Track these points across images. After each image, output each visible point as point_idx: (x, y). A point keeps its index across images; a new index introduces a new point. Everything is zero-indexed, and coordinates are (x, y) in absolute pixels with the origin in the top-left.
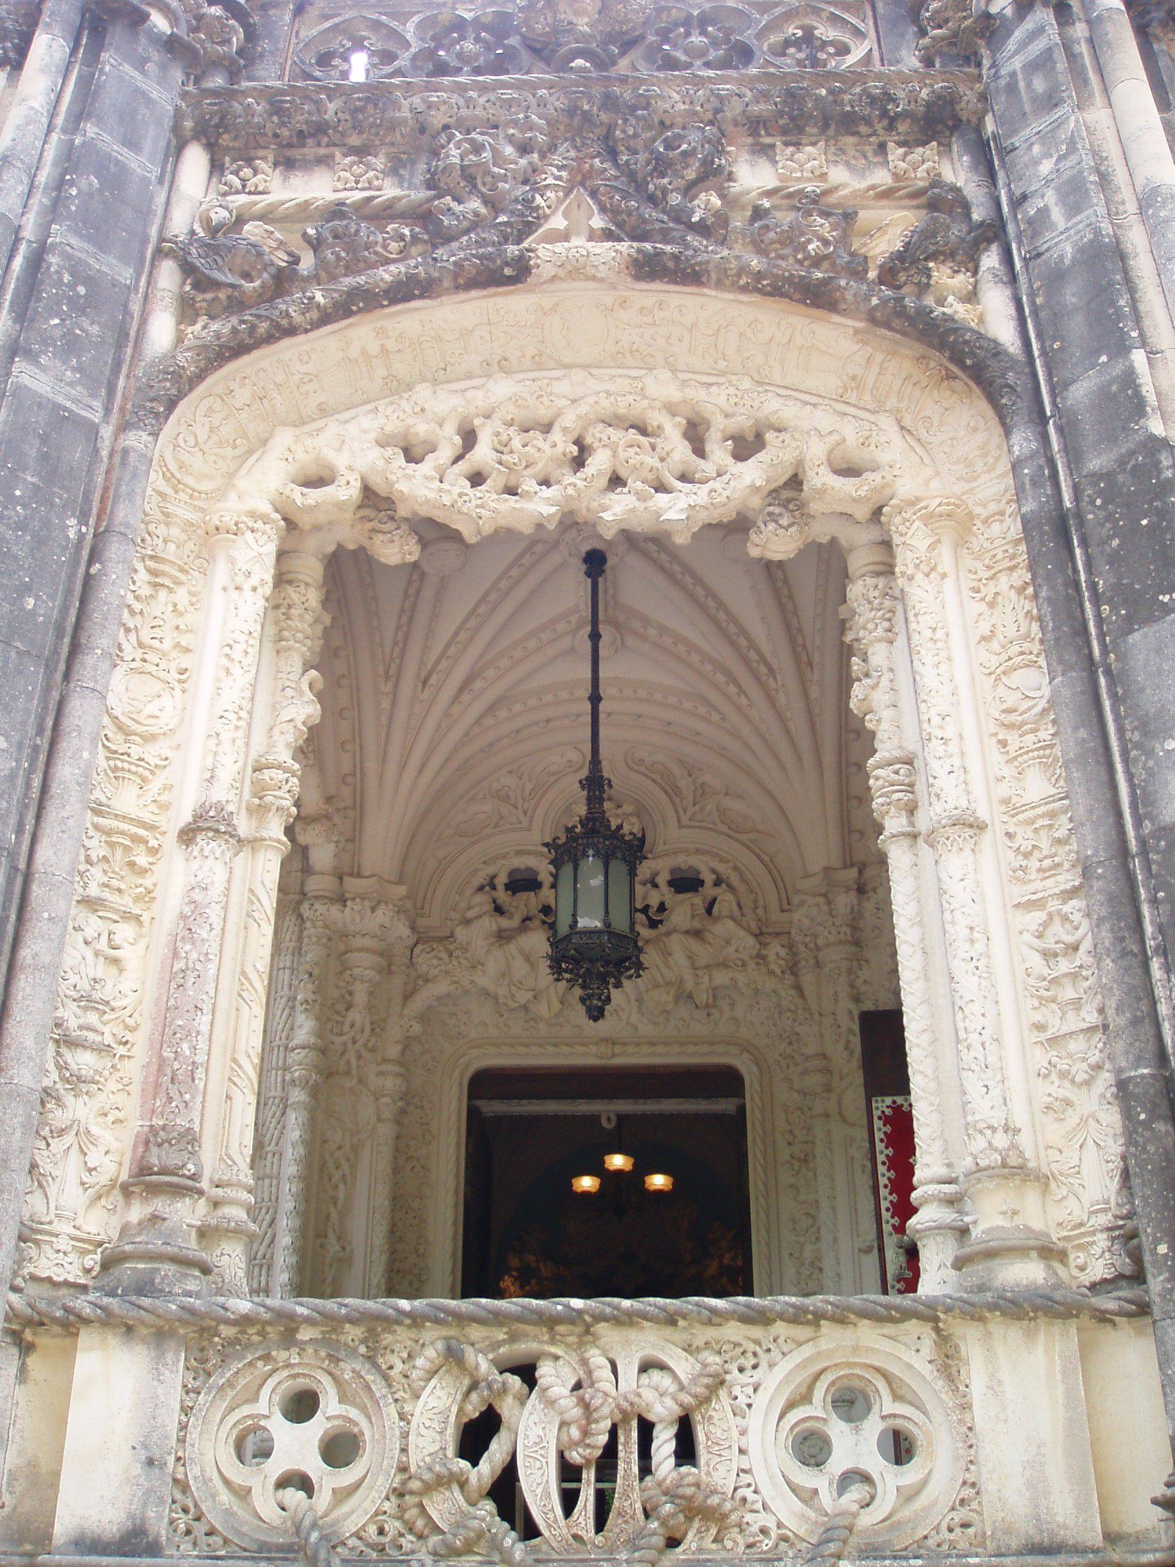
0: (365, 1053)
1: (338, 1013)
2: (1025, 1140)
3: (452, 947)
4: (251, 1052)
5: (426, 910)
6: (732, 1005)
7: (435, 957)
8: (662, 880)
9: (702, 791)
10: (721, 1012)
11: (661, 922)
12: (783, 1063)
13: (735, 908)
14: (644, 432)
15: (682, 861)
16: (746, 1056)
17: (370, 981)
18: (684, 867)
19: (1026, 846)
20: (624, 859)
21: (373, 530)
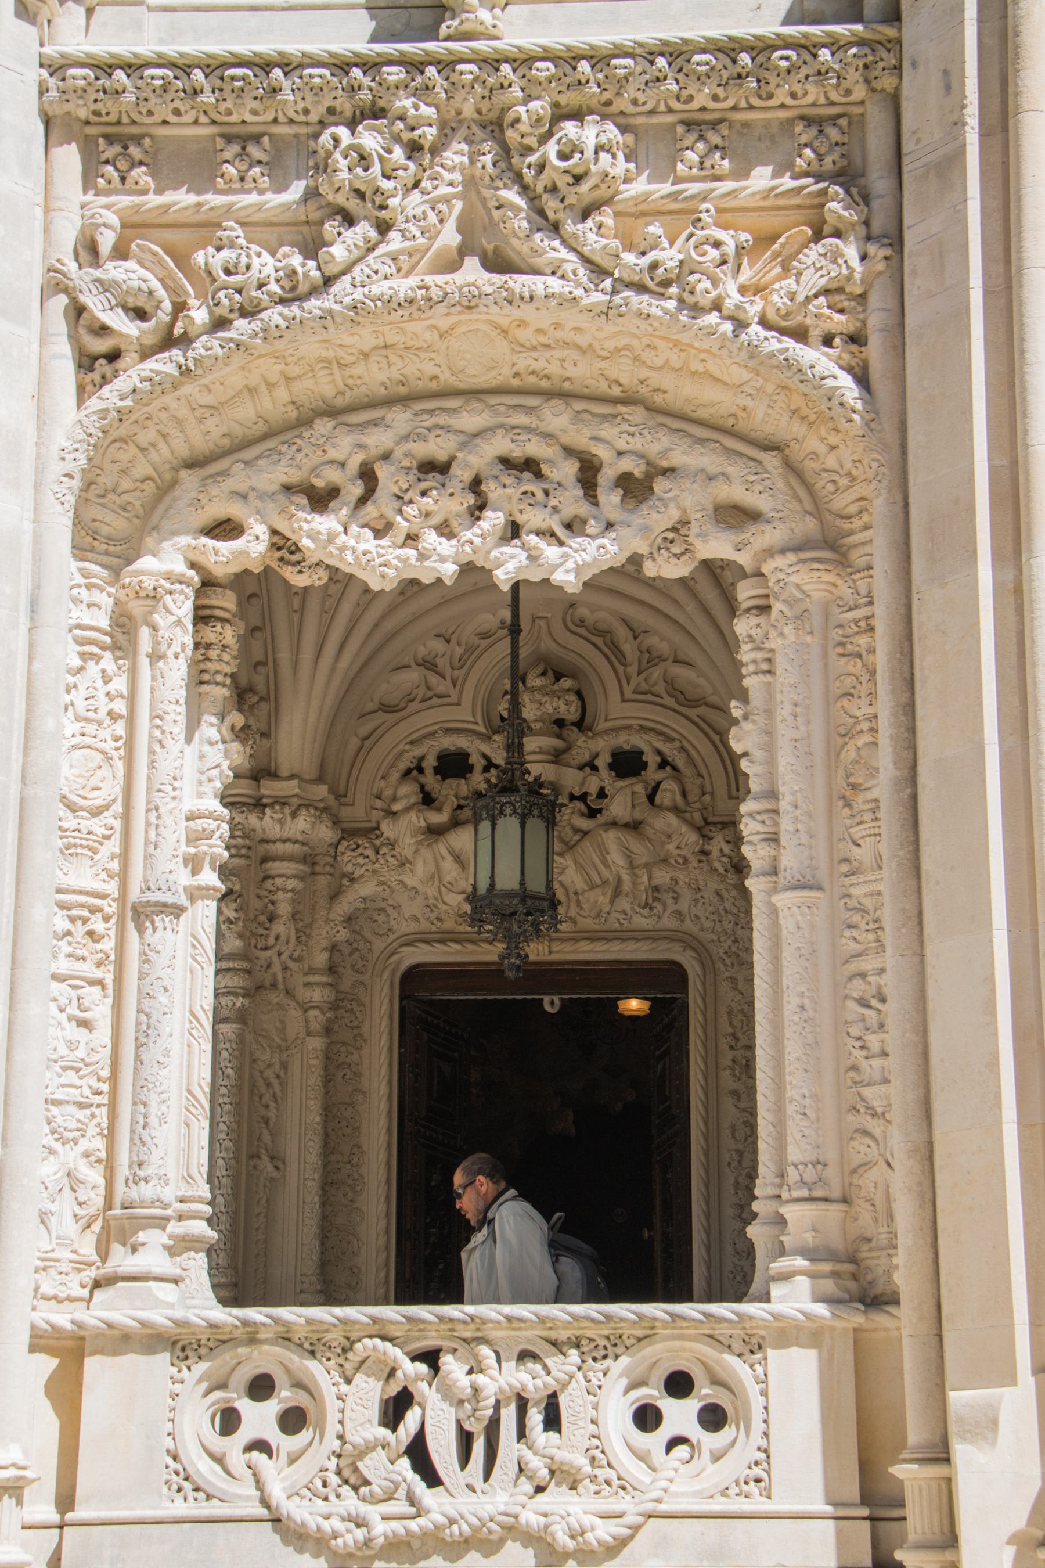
0: (291, 964)
1: (260, 924)
4: (203, 1083)
6: (676, 899)
8: (602, 762)
9: (651, 659)
10: (665, 905)
11: (600, 811)
13: (678, 798)
15: (625, 741)
16: (690, 953)
17: (292, 890)
20: (541, 816)
21: (281, 559)
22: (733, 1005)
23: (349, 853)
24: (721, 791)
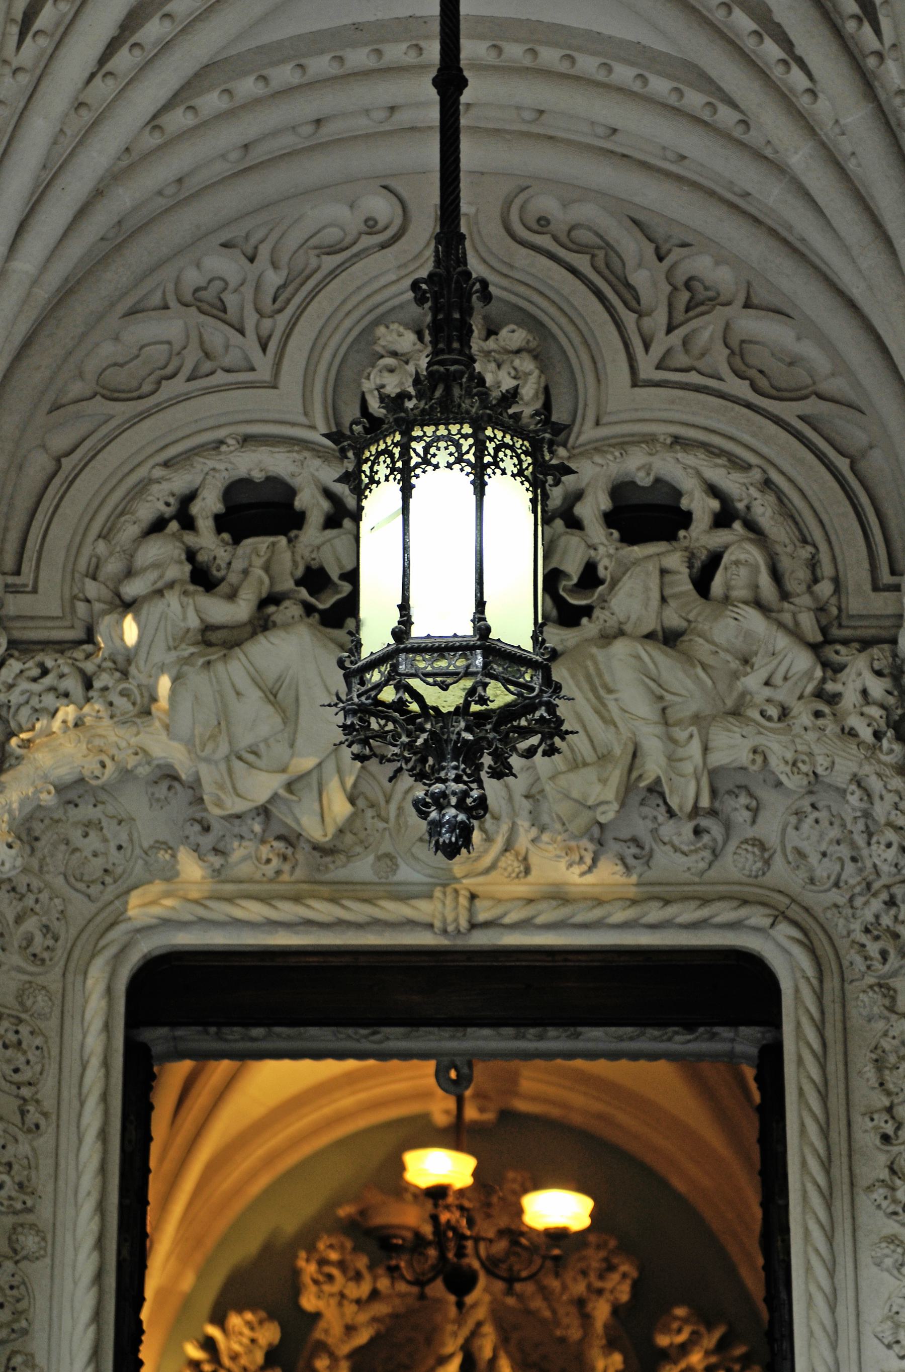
3: (89, 667)
5: (27, 577)
6: (755, 812)
7: (52, 689)
9: (695, 298)
10: (728, 827)
11: (587, 611)
12: (873, 949)
13: (765, 580)
15: (637, 466)
16: (784, 930)
18: (644, 480)
22: (886, 1044)
23: (24, 685)
24: (857, 574)
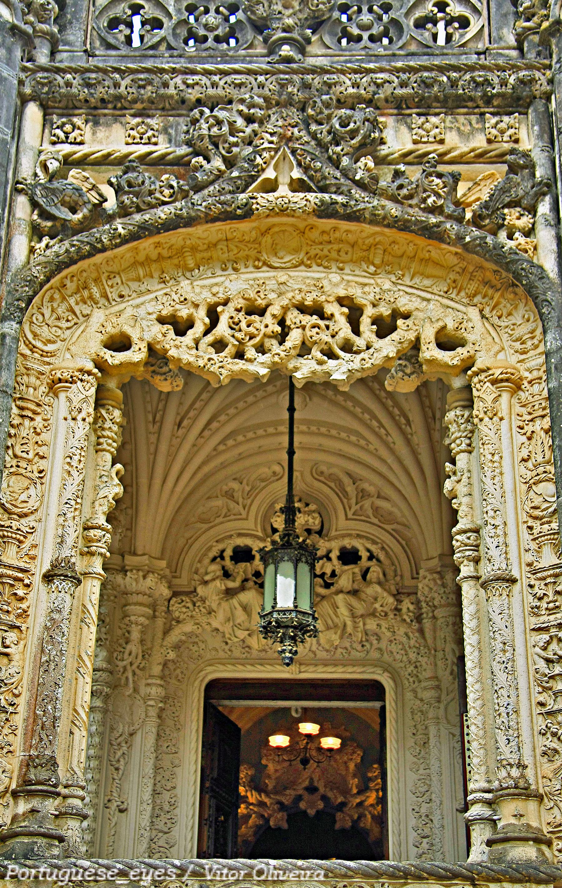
0: (138, 671)
1: (120, 645)
2: (529, 773)
3: (195, 599)
4: (84, 704)
5: (178, 574)
7: (184, 606)
8: (334, 555)
9: (363, 494)
10: (371, 645)
11: (332, 584)
12: (411, 680)
13: (381, 576)
14: (322, 317)
15: (348, 543)
16: (386, 674)
17: (142, 624)
18: (349, 547)
19: (540, 593)
20: (307, 562)
21: (154, 372)
22: (414, 707)
23: (177, 605)
24: (407, 574)
